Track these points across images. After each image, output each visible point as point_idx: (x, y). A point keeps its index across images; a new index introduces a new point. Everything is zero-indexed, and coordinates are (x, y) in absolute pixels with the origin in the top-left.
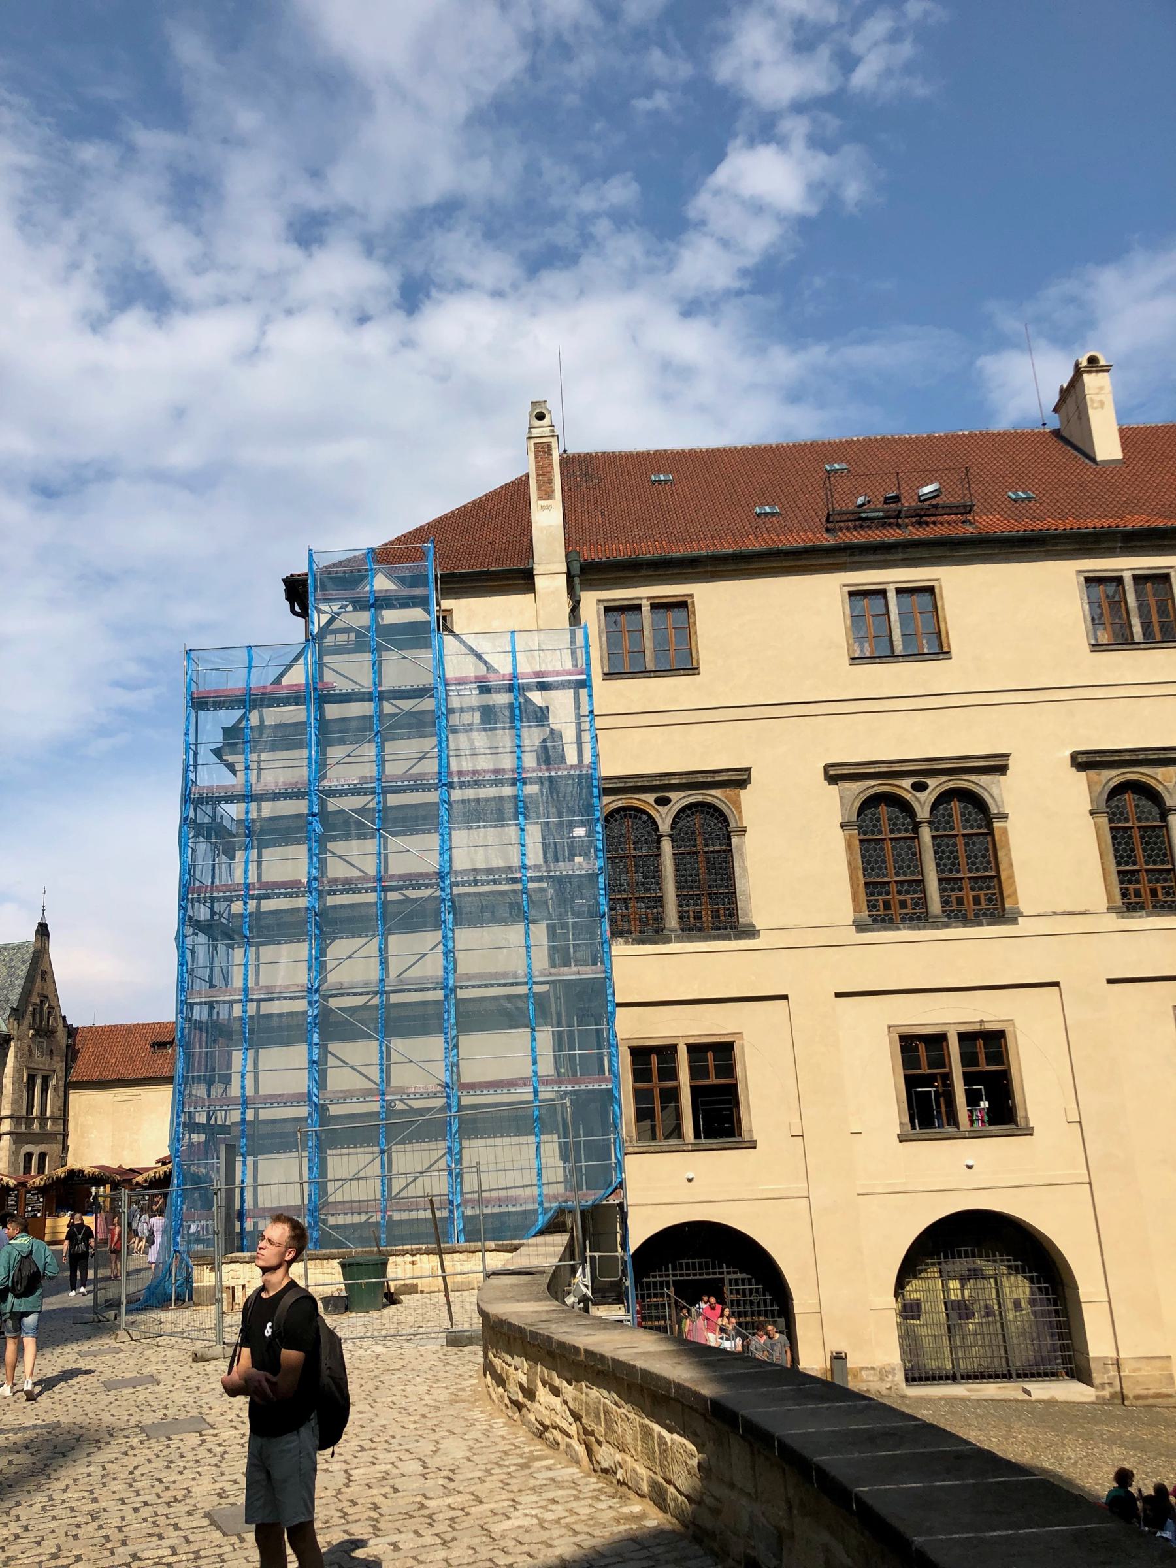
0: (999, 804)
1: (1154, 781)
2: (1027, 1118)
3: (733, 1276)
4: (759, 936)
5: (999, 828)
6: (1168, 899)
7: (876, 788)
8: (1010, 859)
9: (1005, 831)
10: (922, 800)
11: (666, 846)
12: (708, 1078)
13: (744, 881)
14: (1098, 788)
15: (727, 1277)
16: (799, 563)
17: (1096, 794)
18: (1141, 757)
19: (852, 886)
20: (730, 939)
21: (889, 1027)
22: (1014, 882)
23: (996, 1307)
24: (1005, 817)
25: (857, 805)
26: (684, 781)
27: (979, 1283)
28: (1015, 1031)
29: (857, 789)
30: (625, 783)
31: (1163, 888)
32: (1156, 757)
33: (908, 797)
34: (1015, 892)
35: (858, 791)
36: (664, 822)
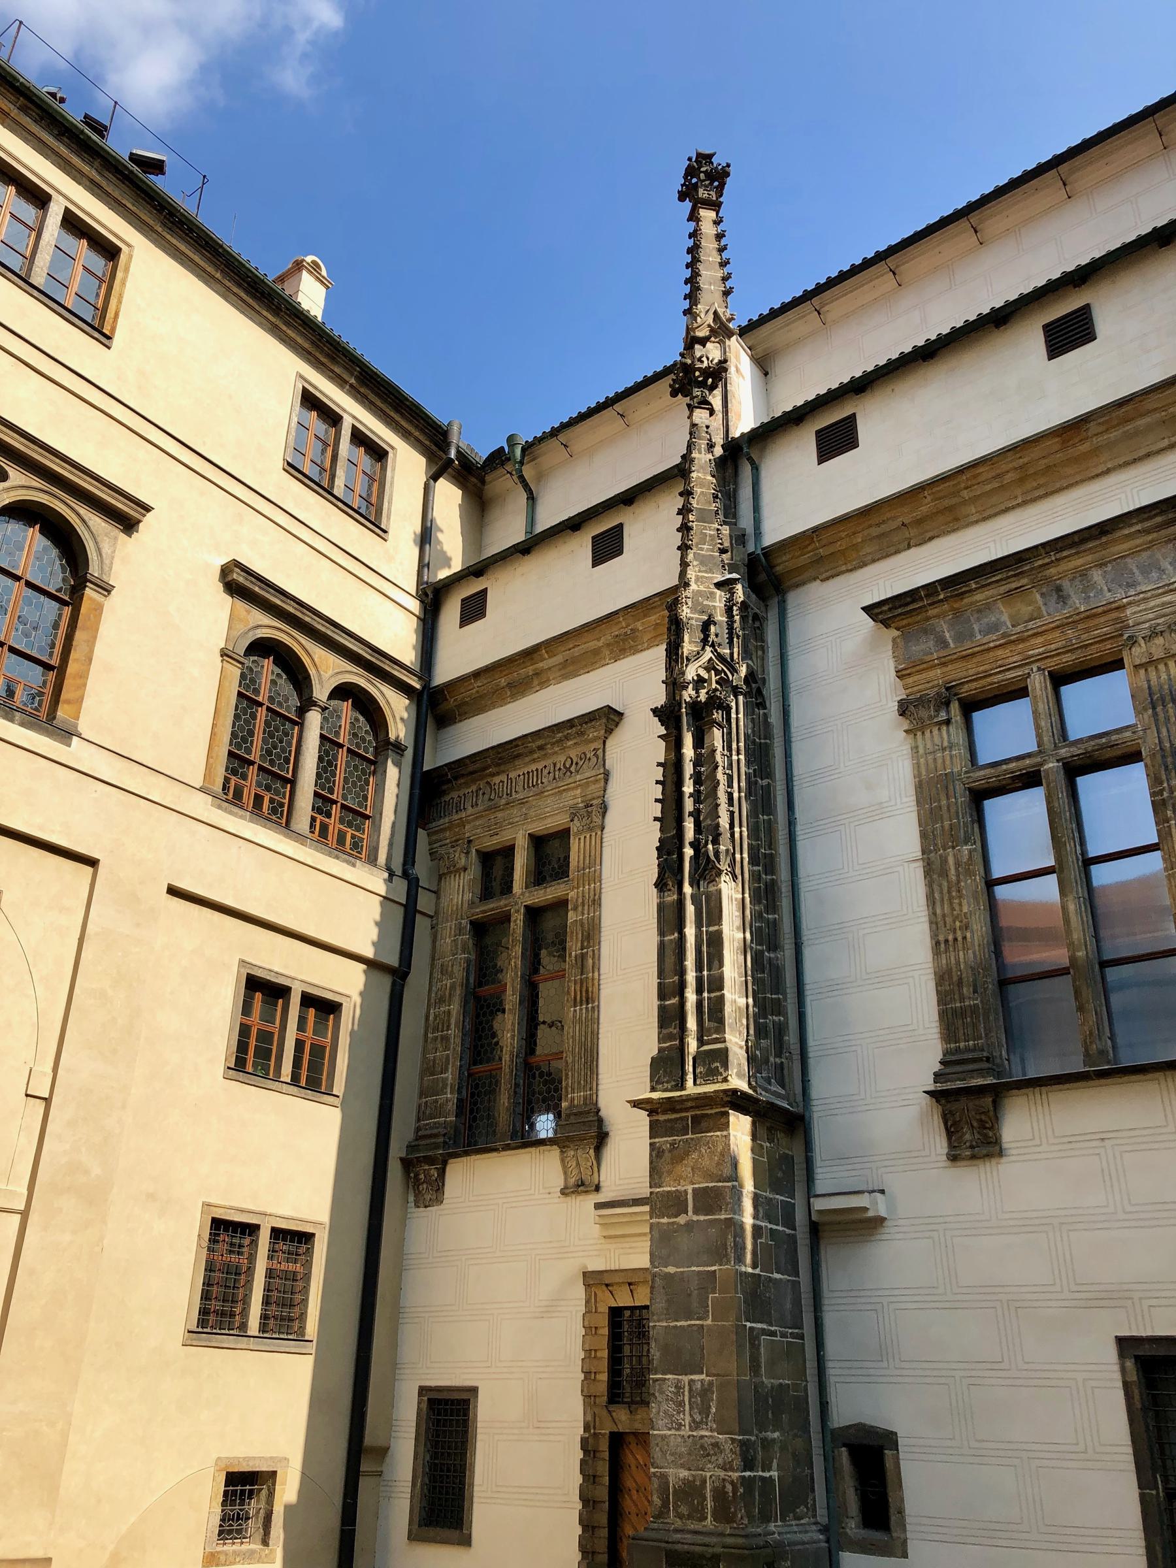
0: (106, 569)
5: (91, 599)
9: (99, 609)
14: (241, 628)
22: (85, 685)
24: (106, 589)
31: (272, 801)
34: (80, 700)
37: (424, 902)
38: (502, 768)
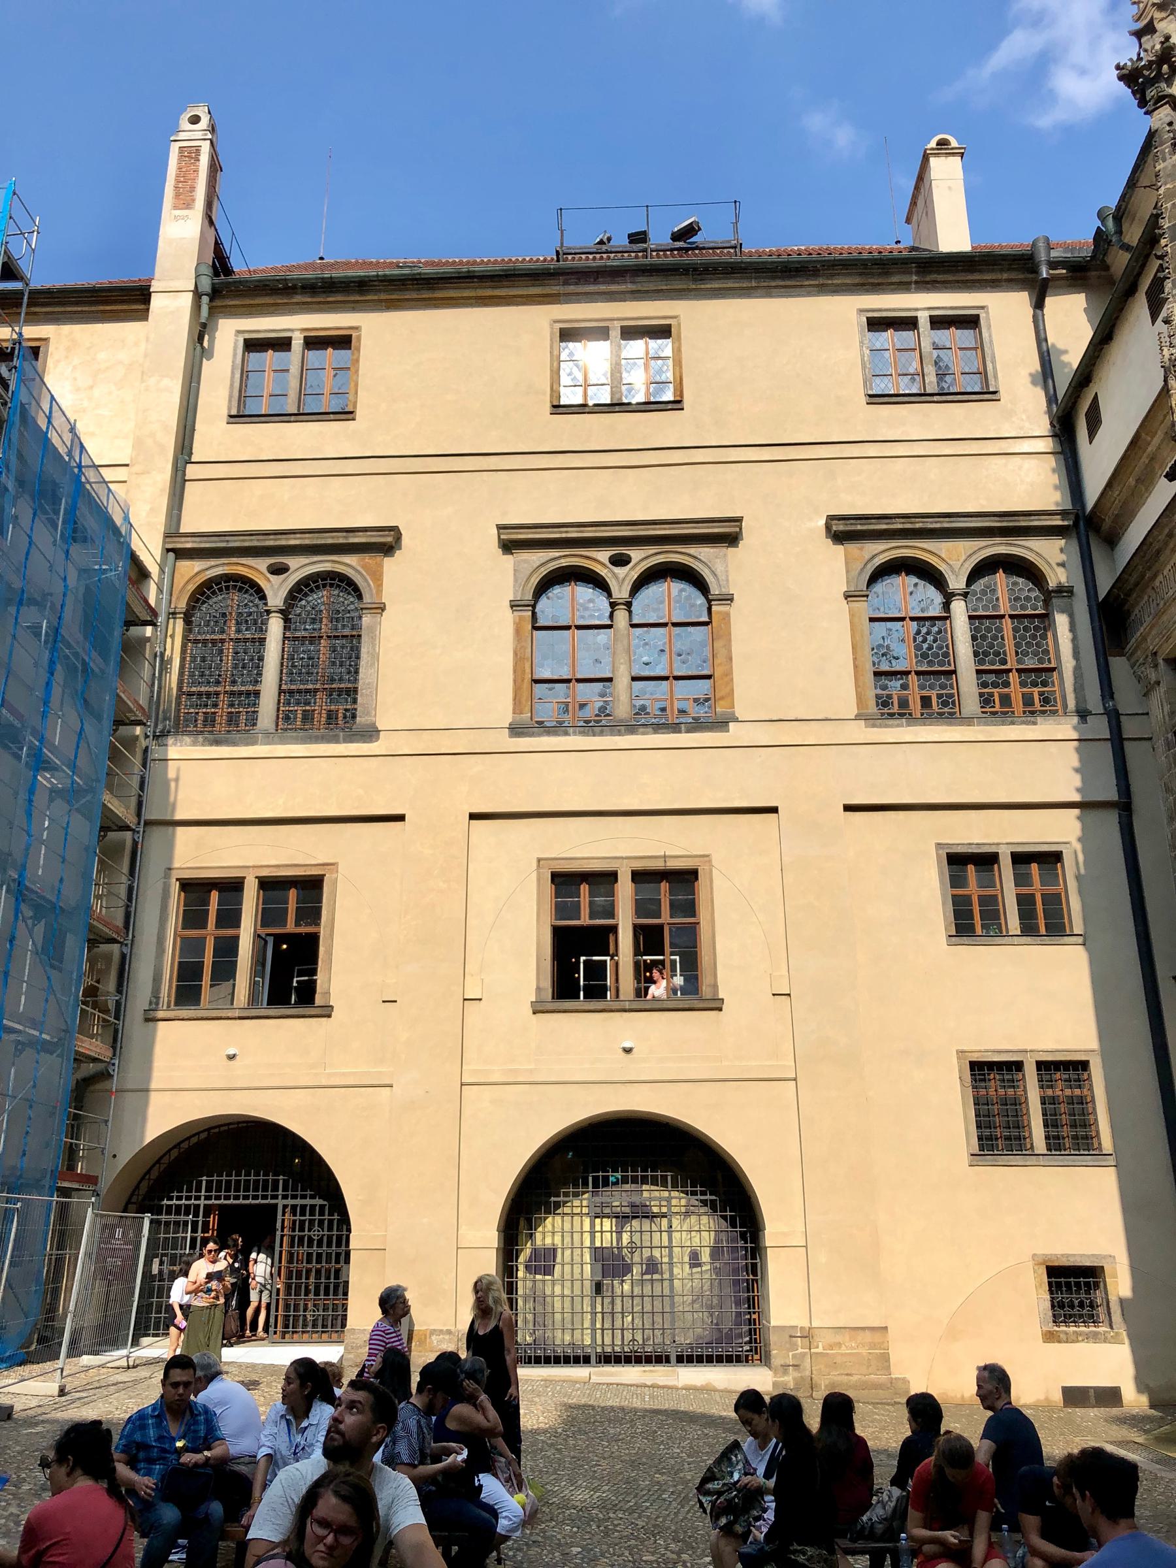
1: (935, 559)
2: (715, 987)
3: (290, 1202)
4: (377, 739)
5: (718, 613)
6: (946, 710)
7: (562, 561)
8: (730, 651)
9: (728, 615)
10: (621, 576)
11: (275, 626)
12: (284, 923)
13: (370, 671)
15: (280, 1202)
16: (497, 292)
17: (855, 573)
18: (918, 526)
19: (515, 681)
20: (337, 742)
21: (539, 860)
23: (666, 1260)
24: (729, 599)
25: (535, 580)
26: (307, 542)
27: (647, 1223)
28: (711, 871)
29: (539, 561)
30: (228, 541)
31: (939, 696)
32: (938, 526)
33: (603, 572)
35: (538, 563)
36: (275, 595)
37: (1130, 728)
38: (1154, 569)
